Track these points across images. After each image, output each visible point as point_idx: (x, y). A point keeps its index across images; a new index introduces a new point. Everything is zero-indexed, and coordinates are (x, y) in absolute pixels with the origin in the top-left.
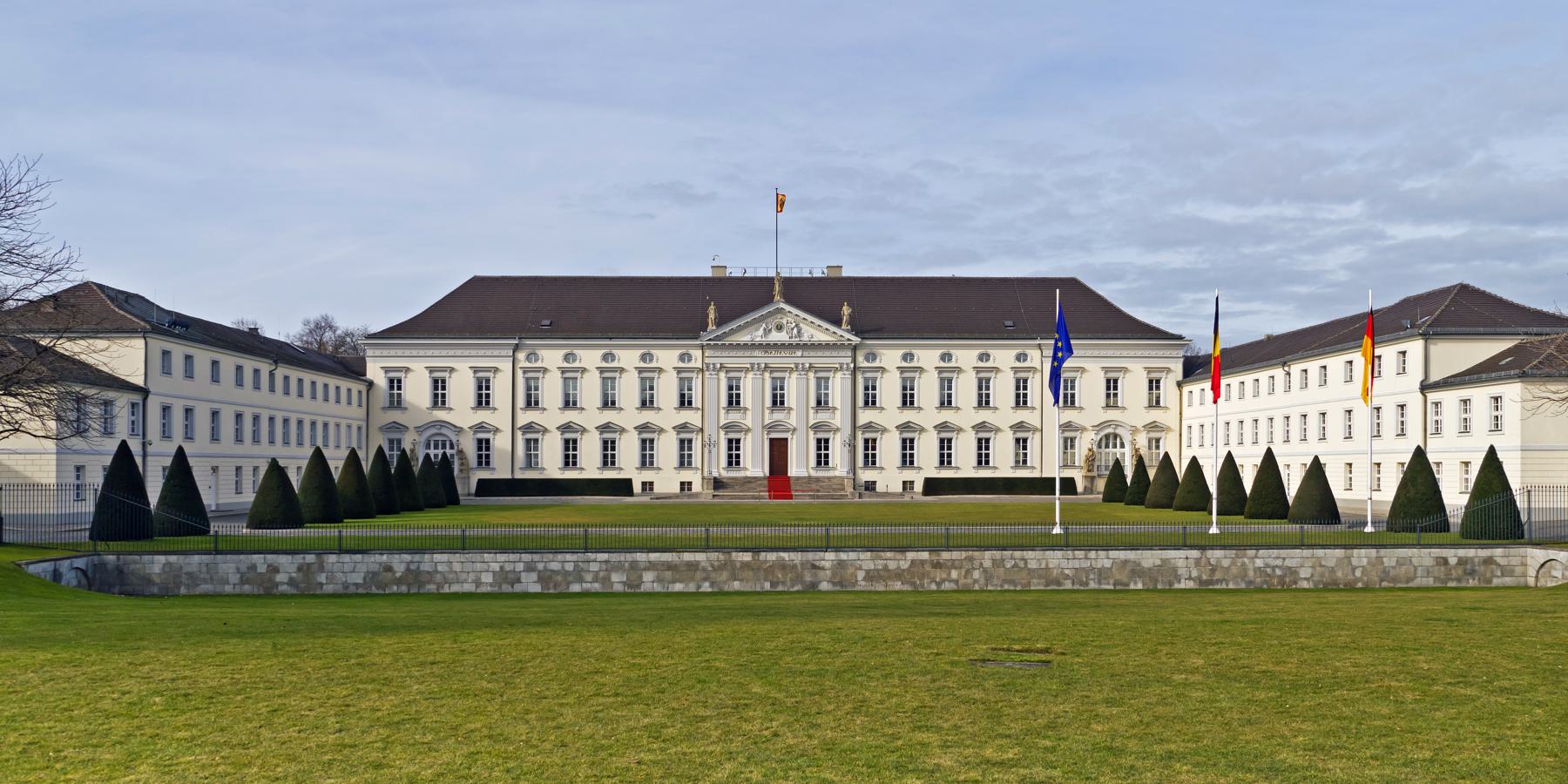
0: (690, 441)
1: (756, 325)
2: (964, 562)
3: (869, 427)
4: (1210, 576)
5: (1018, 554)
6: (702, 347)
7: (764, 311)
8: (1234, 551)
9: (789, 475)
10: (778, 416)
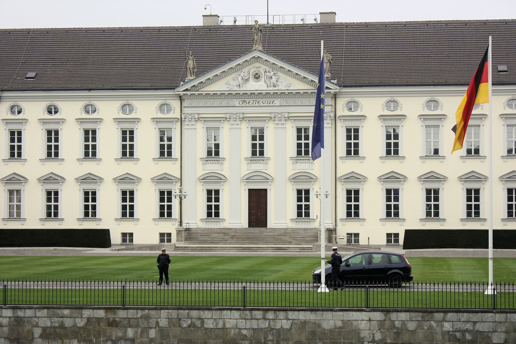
0: (170, 193)
1: (234, 75)
2: (140, 320)
3: (352, 177)
4: (395, 339)
5: (194, 313)
6: (181, 98)
7: (240, 61)
8: (421, 314)
9: (269, 226)
10: (257, 166)
